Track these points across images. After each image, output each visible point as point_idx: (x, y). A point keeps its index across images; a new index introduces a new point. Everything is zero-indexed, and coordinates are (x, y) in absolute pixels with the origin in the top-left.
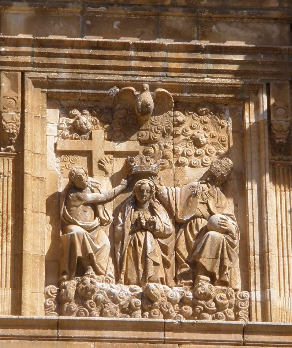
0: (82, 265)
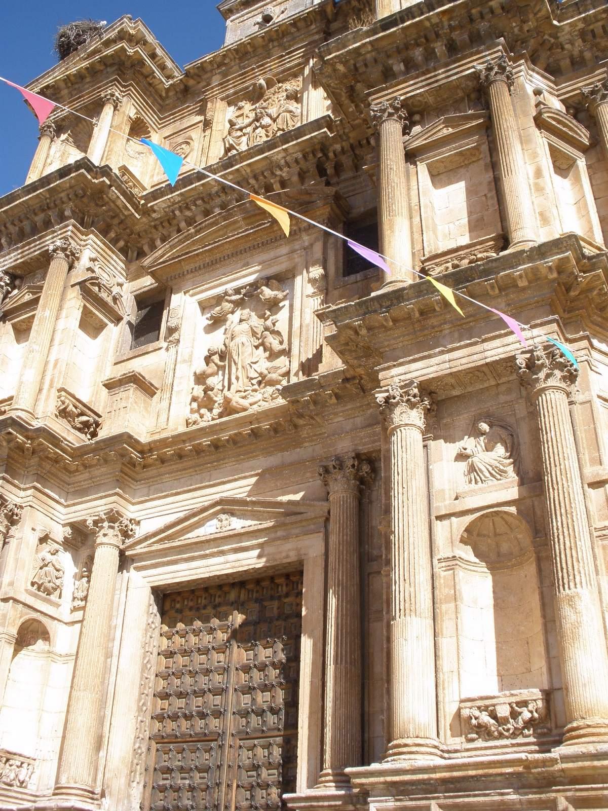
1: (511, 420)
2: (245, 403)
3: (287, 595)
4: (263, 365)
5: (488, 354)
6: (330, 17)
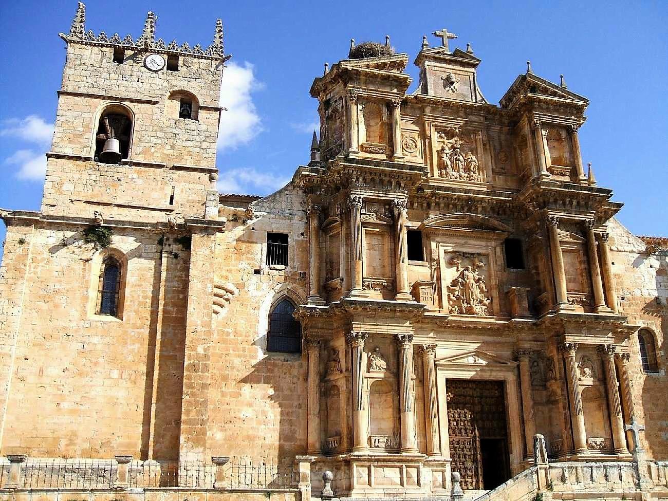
0: (446, 167)
1: (592, 360)
2: (477, 311)
3: (492, 389)
4: (479, 296)
5: (596, 341)
6: (491, 112)
